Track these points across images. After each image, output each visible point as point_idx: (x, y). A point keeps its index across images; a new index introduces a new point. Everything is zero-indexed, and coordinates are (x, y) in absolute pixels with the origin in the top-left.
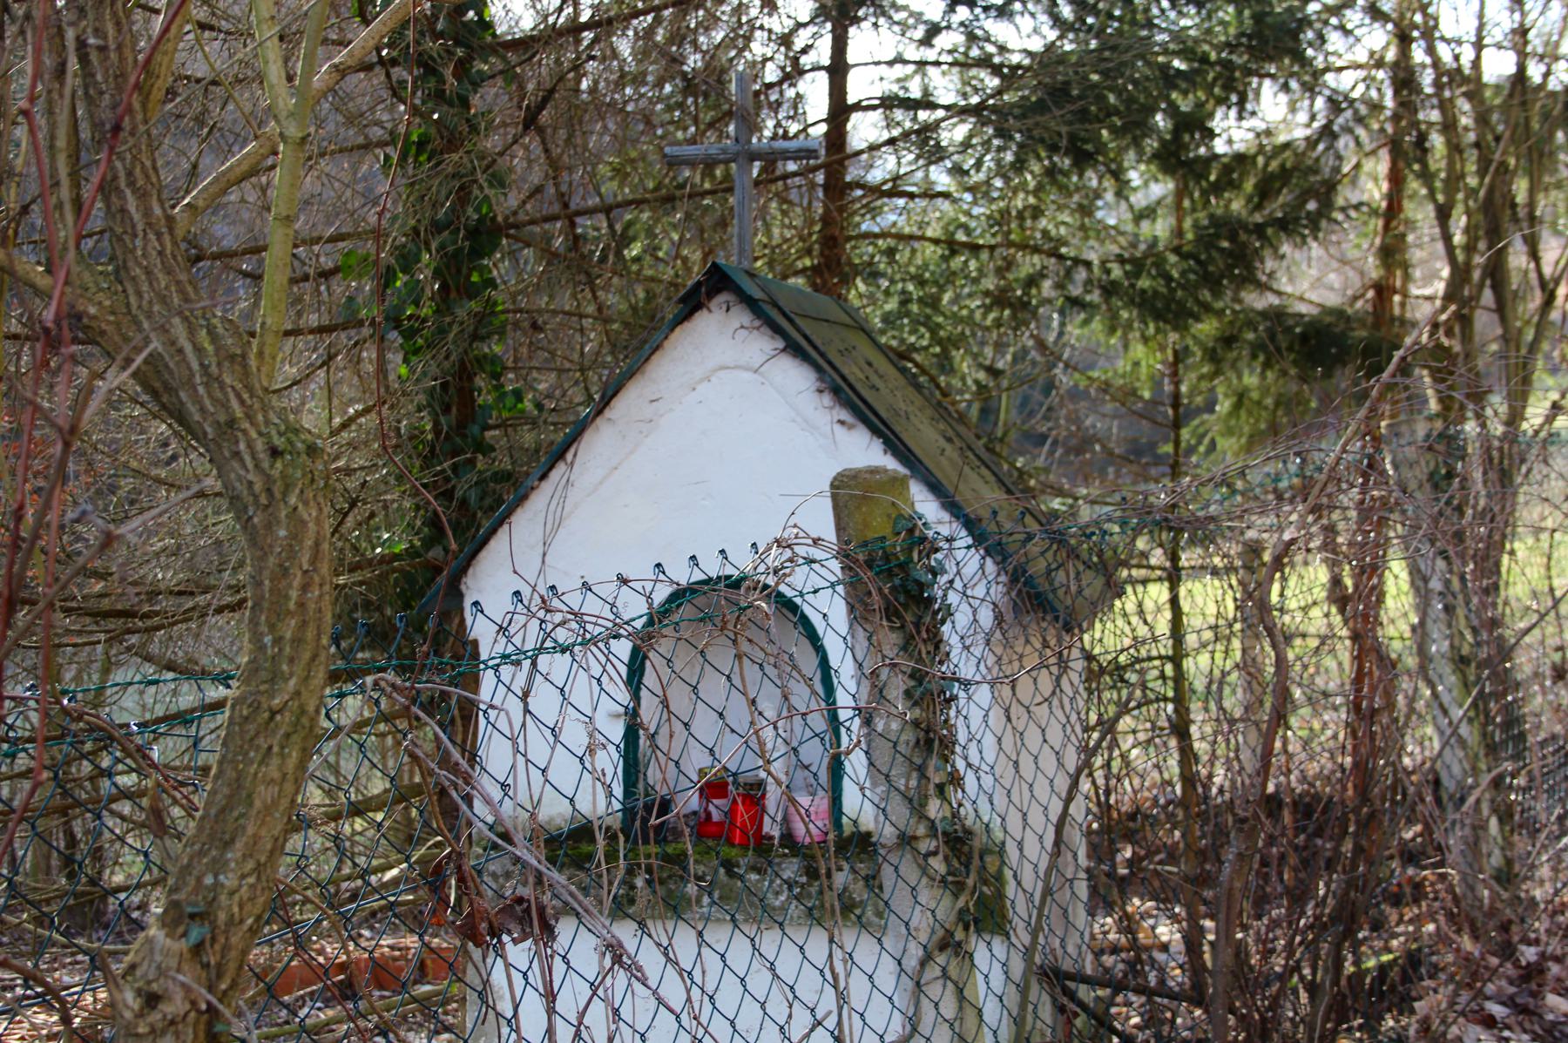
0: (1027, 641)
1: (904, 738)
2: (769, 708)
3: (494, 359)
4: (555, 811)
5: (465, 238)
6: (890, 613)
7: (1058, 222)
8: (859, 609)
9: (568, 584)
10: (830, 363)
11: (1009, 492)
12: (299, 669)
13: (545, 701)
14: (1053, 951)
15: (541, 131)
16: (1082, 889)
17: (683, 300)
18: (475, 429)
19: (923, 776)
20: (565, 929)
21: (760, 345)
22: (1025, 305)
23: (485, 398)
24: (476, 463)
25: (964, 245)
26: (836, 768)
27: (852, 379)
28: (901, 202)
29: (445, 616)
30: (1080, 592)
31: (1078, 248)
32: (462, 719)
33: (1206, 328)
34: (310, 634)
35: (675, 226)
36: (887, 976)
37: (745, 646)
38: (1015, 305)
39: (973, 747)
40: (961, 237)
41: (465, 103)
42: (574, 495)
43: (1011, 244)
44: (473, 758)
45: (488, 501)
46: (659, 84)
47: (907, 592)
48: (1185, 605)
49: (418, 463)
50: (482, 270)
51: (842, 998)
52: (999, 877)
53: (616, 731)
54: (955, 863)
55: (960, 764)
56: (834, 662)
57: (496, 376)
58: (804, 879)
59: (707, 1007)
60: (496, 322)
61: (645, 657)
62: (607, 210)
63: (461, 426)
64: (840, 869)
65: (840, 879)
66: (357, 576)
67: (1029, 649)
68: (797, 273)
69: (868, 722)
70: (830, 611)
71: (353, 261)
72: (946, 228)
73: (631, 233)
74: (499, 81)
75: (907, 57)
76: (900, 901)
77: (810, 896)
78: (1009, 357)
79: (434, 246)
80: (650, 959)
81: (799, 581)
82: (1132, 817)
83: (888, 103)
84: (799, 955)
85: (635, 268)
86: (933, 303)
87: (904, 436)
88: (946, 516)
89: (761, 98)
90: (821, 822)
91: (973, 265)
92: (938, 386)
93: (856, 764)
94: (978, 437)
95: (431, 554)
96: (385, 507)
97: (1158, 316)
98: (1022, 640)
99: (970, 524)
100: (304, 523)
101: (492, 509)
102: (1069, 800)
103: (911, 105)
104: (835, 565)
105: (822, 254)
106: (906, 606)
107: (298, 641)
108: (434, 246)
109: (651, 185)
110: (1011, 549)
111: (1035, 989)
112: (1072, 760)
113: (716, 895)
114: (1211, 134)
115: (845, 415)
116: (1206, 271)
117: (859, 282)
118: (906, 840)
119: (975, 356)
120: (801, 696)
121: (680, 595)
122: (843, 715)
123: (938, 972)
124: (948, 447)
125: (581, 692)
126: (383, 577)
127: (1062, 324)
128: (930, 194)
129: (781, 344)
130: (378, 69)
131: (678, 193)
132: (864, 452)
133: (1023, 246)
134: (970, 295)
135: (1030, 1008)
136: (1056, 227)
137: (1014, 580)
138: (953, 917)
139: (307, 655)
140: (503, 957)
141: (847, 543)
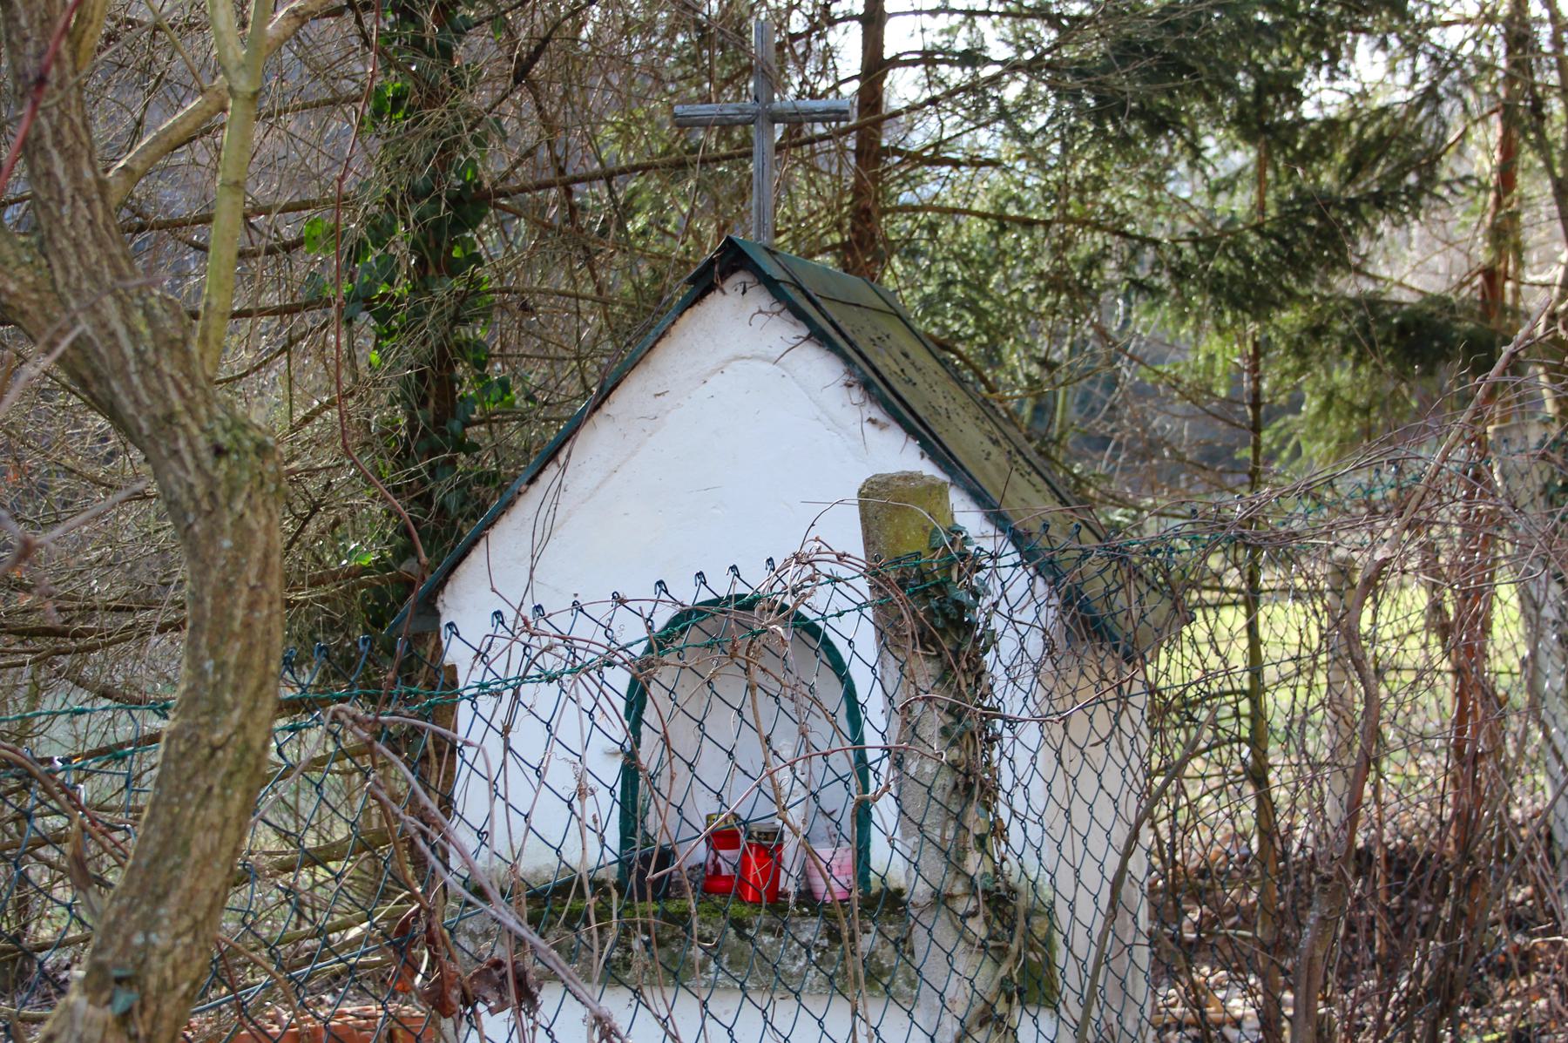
0: (1082, 673)
1: (939, 782)
2: (786, 746)
3: (478, 346)
4: (538, 863)
5: (447, 207)
6: (925, 639)
7: (1123, 195)
8: (889, 636)
10: (860, 354)
11: (1063, 502)
12: (244, 698)
13: (528, 737)
15: (533, 86)
16: (1143, 956)
18: (456, 425)
20: (549, 997)
21: (781, 332)
23: (467, 390)
24: (455, 465)
25: (1015, 220)
26: (863, 815)
27: (885, 372)
28: (945, 170)
29: (419, 638)
30: (1142, 617)
31: (1146, 226)
32: (437, 758)
33: (1290, 318)
34: (257, 659)
35: (685, 198)
37: (758, 677)
38: (1073, 288)
40: (1012, 210)
41: (447, 53)
43: (1068, 220)
44: (447, 804)
45: (468, 509)
46: (670, 35)
48: (1264, 633)
49: (389, 464)
52: (1048, 942)
53: (610, 771)
55: (1004, 812)
56: (861, 698)
57: (480, 365)
58: (825, 942)
60: (481, 304)
62: (608, 176)
63: (439, 421)
65: (866, 943)
66: (321, 592)
68: (823, 251)
69: (898, 764)
70: (857, 637)
71: (318, 231)
72: (995, 200)
73: (636, 204)
74: (487, 28)
76: (934, 969)
77: (831, 961)
78: (1066, 349)
81: (820, 601)
82: (1202, 873)
83: (927, 58)
85: (640, 243)
86: (980, 286)
87: (943, 437)
88: (990, 529)
89: (788, 49)
91: (1026, 241)
92: (984, 380)
93: (885, 811)
94: (1029, 439)
95: (403, 567)
96: (352, 514)
97: (1236, 304)
98: (1076, 672)
99: (1018, 538)
100: (251, 532)
102: (1127, 854)
104: (863, 584)
105: (853, 229)
107: (243, 667)
108: (412, 216)
110: (1065, 567)
112: (1131, 808)
113: (725, 958)
114: (1298, 97)
115: (876, 413)
116: (1292, 253)
117: (896, 261)
118: (941, 899)
119: (1027, 347)
120: (821, 732)
121: (685, 618)
122: (872, 755)
124: (994, 450)
125: (571, 726)
126: (349, 593)
127: (1128, 312)
128: (975, 162)
129: (804, 332)
130: (349, 14)
131: (689, 158)
132: (898, 455)
133: (1082, 223)
134: (1021, 277)
137: (1067, 603)
138: (994, 988)
139: (253, 684)
140: (479, 1028)
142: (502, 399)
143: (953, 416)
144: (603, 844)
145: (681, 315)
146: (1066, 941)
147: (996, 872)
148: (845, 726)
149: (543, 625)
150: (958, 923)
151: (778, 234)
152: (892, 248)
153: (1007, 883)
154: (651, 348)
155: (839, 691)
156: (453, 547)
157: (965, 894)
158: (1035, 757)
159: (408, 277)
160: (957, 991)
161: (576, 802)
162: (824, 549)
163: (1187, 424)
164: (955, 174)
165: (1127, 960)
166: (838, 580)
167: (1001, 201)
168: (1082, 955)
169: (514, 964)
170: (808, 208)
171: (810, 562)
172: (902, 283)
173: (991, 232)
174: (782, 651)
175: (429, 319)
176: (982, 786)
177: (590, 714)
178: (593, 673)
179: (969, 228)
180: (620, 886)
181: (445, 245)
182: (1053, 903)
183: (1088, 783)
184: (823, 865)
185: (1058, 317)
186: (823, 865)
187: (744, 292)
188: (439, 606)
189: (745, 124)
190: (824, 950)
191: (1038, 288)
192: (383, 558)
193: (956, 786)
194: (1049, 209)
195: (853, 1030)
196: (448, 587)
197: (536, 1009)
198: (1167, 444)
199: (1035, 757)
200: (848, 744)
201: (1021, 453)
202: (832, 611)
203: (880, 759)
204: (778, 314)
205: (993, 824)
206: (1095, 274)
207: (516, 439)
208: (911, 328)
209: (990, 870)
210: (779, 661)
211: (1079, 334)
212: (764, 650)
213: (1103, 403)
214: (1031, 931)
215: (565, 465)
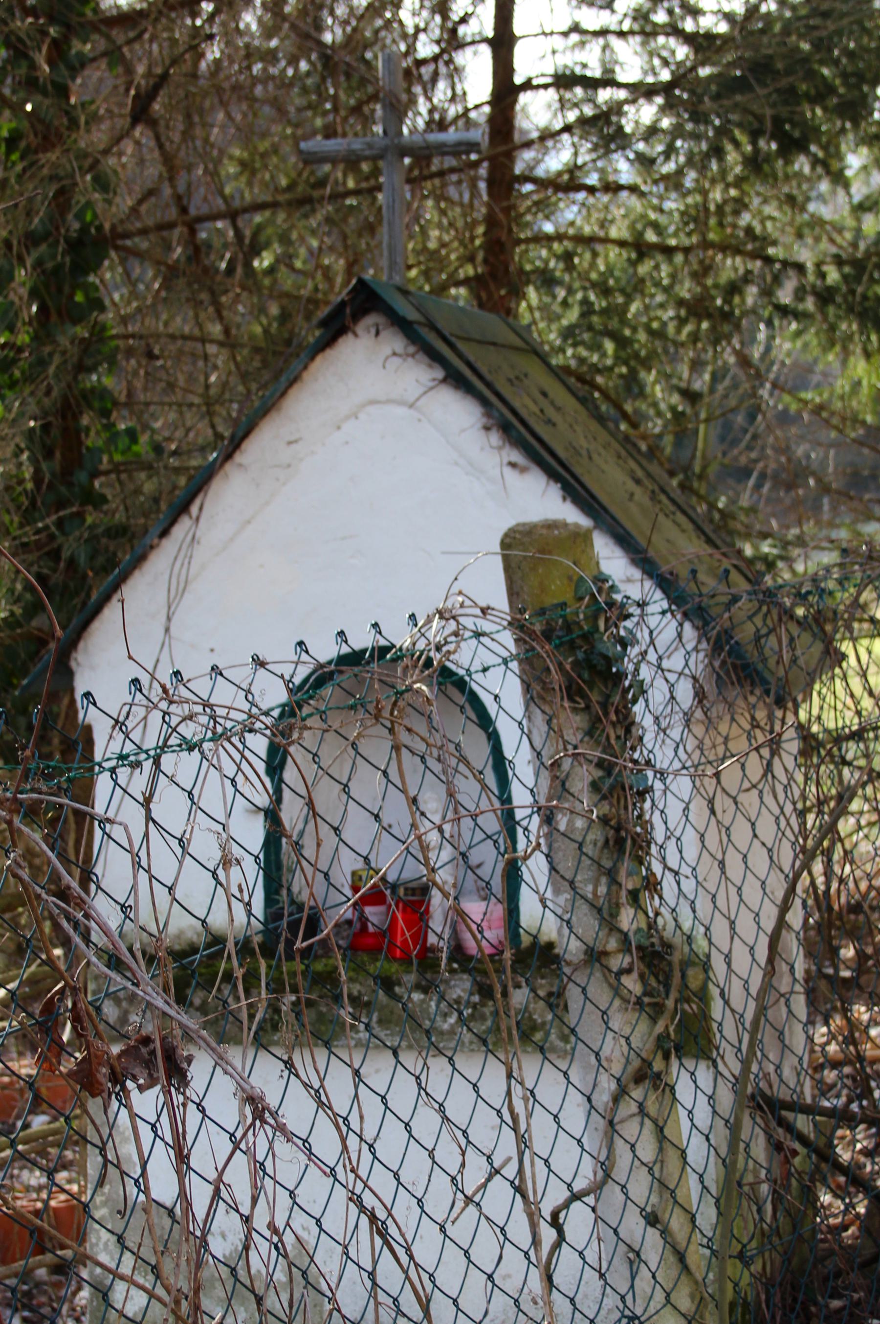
0: (733, 719)
1: (590, 837)
2: (433, 802)
3: (102, 393)
4: (182, 926)
6: (572, 692)
7: (764, 213)
8: (535, 689)
9: (195, 667)
11: (709, 541)
13: (170, 807)
14: (767, 1076)
17: (324, 323)
19: (614, 881)
20: (200, 1069)
21: (415, 376)
22: (726, 316)
23: (93, 440)
26: (512, 876)
28: (581, 196)
29: (53, 697)
30: (794, 660)
31: (788, 247)
32: (74, 830)
35: (313, 232)
36: (575, 1116)
37: (404, 737)
39: (671, 845)
40: (651, 237)
41: (63, 92)
42: (200, 554)
43: (706, 244)
44: (87, 877)
45: (100, 560)
46: (293, 61)
47: (592, 668)
49: (16, 519)
50: (88, 288)
51: (523, 1142)
52: (703, 996)
53: (252, 834)
54: (653, 982)
55: (657, 868)
56: (508, 753)
57: (105, 413)
58: (476, 998)
59: (366, 1156)
60: (105, 350)
61: (286, 752)
62: (232, 215)
63: (66, 473)
64: (518, 986)
65: (520, 997)
67: (735, 731)
68: (458, 284)
69: (548, 819)
70: (503, 690)
72: (632, 227)
73: (262, 238)
74: (103, 64)
75: (585, 25)
76: (589, 1028)
77: (483, 1018)
78: (707, 377)
79: (29, 263)
80: (297, 1110)
81: (465, 657)
82: (856, 908)
84: (470, 1087)
87: (586, 480)
88: (637, 574)
89: (415, 75)
90: (494, 934)
92: (625, 416)
93: (536, 869)
94: (672, 474)
95: (34, 623)
98: (728, 718)
99: (666, 583)
101: (106, 569)
102: (785, 908)
103: (591, 84)
104: (507, 638)
105: (486, 261)
106: (591, 685)
108: (29, 263)
109: (284, 182)
110: (714, 612)
111: (747, 1122)
112: (787, 856)
113: (375, 1018)
115: (516, 456)
117: (532, 293)
118: (595, 956)
119: (668, 377)
120: (468, 790)
122: (519, 814)
123: (634, 1108)
124: (638, 491)
125: (212, 797)
127: (771, 338)
128: (612, 188)
129: (440, 374)
131: (316, 194)
132: (540, 501)
134: (662, 306)
135: (742, 1146)
136: (762, 222)
137: (716, 648)
138: (650, 1045)
140: (129, 1107)
141: (522, 611)
142: (129, 448)
143: (595, 456)
144: (249, 913)
145: (312, 358)
146: (722, 994)
147: (650, 927)
148: (491, 780)
149: (184, 692)
150: (612, 980)
151: (409, 267)
152: (525, 278)
153: (661, 938)
154: (284, 394)
155: (485, 749)
156: (84, 604)
157: (619, 951)
158: (687, 808)
159: (30, 323)
160: (613, 1050)
161: (221, 872)
162: (468, 603)
163: (832, 453)
164: (591, 200)
165: (784, 1010)
166: (484, 634)
167: (639, 226)
168: (739, 1009)
169: (163, 1039)
170: (440, 239)
171: (454, 618)
172: (537, 315)
173: (629, 260)
174: (429, 708)
175: (51, 370)
176: (634, 841)
177: (233, 781)
178: (235, 740)
179: (606, 256)
180: (268, 950)
181: (67, 289)
182: (708, 956)
183: (741, 833)
184: (474, 927)
185: (699, 345)
186: (474, 927)
187: (377, 333)
188: (73, 664)
189: (374, 159)
190: (474, 1007)
191: (678, 317)
192: (12, 614)
193: (607, 841)
194: (689, 235)
195: (509, 1093)
196: (81, 645)
197: (187, 1084)
198: (813, 474)
199: (687, 808)
200: (497, 804)
201: (663, 491)
202: (476, 666)
203: (530, 816)
204: (413, 356)
205: (646, 878)
206: (737, 300)
207: (149, 487)
208: (548, 365)
209: (644, 926)
210: (424, 720)
211: (720, 363)
212: (409, 710)
213: (746, 431)
214: (687, 987)
215: (198, 519)
